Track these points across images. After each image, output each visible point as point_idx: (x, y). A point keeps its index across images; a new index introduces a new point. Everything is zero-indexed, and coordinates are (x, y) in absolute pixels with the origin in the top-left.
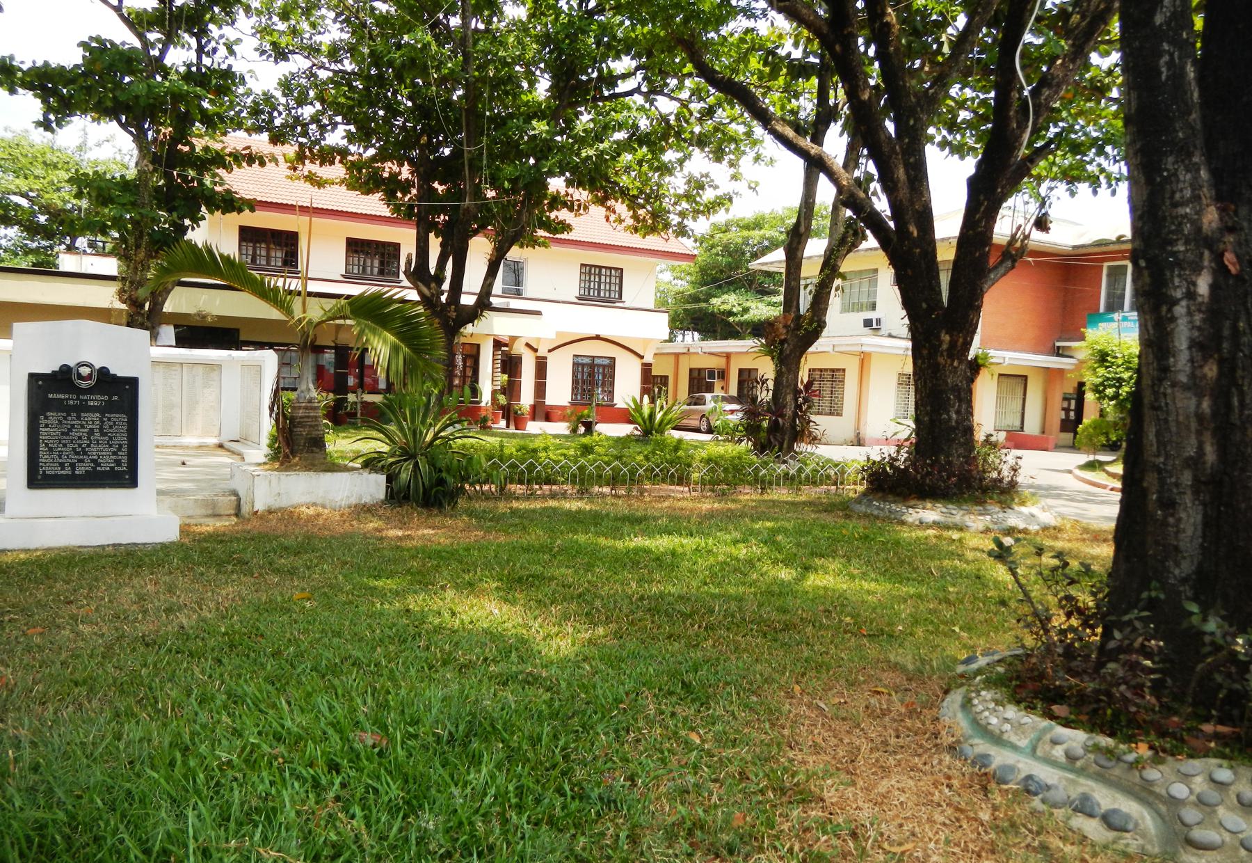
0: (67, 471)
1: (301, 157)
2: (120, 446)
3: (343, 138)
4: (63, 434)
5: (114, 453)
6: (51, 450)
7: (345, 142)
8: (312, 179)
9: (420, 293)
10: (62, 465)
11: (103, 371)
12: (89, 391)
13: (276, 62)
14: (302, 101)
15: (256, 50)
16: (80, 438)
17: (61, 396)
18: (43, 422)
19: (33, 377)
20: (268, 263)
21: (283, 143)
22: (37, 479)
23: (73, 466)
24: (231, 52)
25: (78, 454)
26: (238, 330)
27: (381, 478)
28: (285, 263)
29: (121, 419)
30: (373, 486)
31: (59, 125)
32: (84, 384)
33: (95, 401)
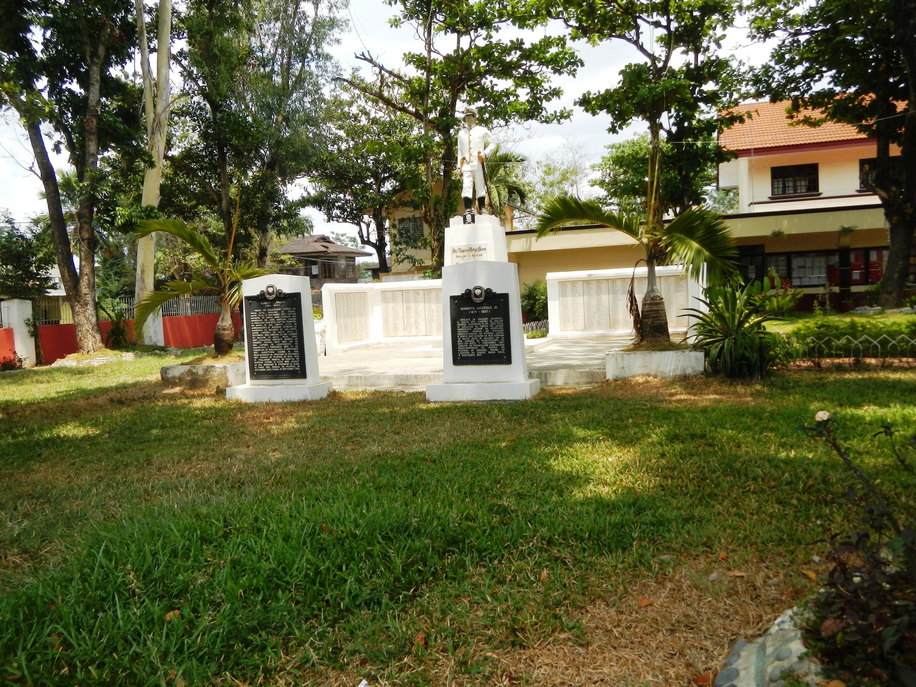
1: (796, 107)
3: (829, 83)
4: (470, 331)
5: (497, 343)
6: (464, 341)
7: (831, 86)
8: (807, 121)
9: (881, 198)
10: (470, 350)
11: (488, 292)
12: (481, 304)
13: (765, 40)
14: (792, 64)
15: (749, 36)
17: (467, 309)
18: (459, 325)
19: (452, 297)
20: (795, 192)
21: (781, 100)
22: (459, 359)
23: (475, 350)
24: (719, 46)
25: (477, 343)
26: (763, 246)
27: (701, 355)
28: (809, 190)
29: (499, 320)
30: (694, 362)
31: (621, 127)
32: (478, 300)
33: (485, 310)
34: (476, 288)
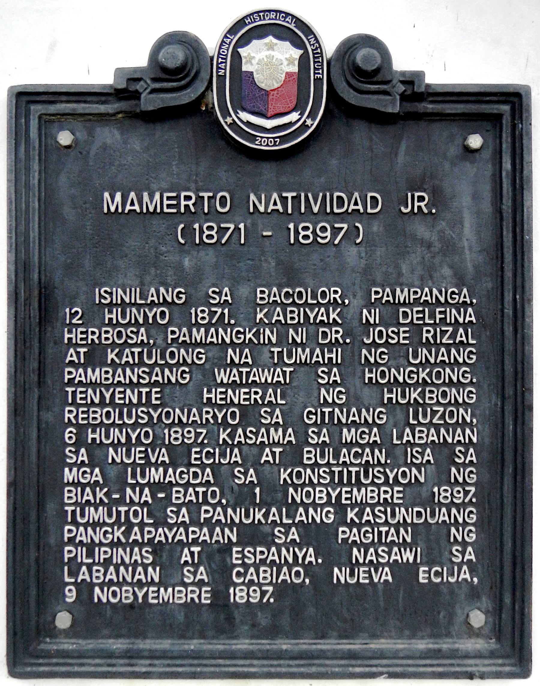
0: (191, 590)
2: (445, 453)
5: (418, 496)
6: (117, 482)
10: (164, 555)
16: (249, 414)
18: (76, 336)
19: (25, 99)
23: (217, 558)
25: (242, 498)
34: (249, 29)
